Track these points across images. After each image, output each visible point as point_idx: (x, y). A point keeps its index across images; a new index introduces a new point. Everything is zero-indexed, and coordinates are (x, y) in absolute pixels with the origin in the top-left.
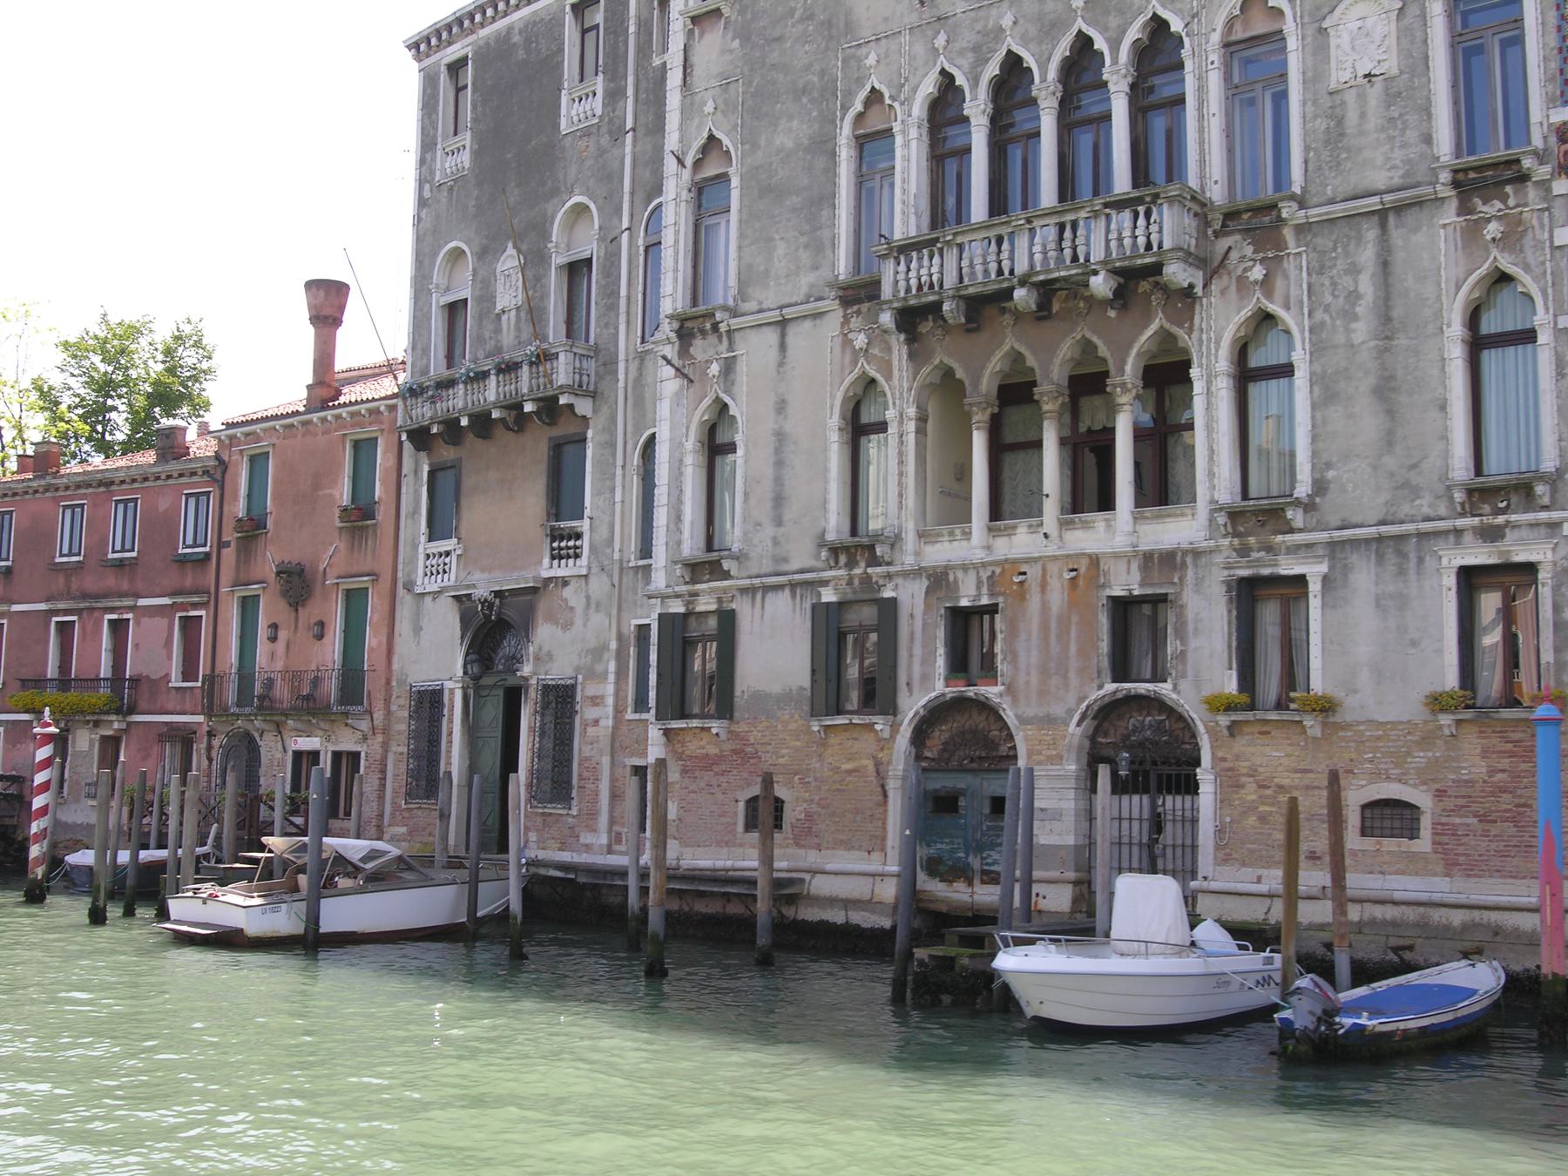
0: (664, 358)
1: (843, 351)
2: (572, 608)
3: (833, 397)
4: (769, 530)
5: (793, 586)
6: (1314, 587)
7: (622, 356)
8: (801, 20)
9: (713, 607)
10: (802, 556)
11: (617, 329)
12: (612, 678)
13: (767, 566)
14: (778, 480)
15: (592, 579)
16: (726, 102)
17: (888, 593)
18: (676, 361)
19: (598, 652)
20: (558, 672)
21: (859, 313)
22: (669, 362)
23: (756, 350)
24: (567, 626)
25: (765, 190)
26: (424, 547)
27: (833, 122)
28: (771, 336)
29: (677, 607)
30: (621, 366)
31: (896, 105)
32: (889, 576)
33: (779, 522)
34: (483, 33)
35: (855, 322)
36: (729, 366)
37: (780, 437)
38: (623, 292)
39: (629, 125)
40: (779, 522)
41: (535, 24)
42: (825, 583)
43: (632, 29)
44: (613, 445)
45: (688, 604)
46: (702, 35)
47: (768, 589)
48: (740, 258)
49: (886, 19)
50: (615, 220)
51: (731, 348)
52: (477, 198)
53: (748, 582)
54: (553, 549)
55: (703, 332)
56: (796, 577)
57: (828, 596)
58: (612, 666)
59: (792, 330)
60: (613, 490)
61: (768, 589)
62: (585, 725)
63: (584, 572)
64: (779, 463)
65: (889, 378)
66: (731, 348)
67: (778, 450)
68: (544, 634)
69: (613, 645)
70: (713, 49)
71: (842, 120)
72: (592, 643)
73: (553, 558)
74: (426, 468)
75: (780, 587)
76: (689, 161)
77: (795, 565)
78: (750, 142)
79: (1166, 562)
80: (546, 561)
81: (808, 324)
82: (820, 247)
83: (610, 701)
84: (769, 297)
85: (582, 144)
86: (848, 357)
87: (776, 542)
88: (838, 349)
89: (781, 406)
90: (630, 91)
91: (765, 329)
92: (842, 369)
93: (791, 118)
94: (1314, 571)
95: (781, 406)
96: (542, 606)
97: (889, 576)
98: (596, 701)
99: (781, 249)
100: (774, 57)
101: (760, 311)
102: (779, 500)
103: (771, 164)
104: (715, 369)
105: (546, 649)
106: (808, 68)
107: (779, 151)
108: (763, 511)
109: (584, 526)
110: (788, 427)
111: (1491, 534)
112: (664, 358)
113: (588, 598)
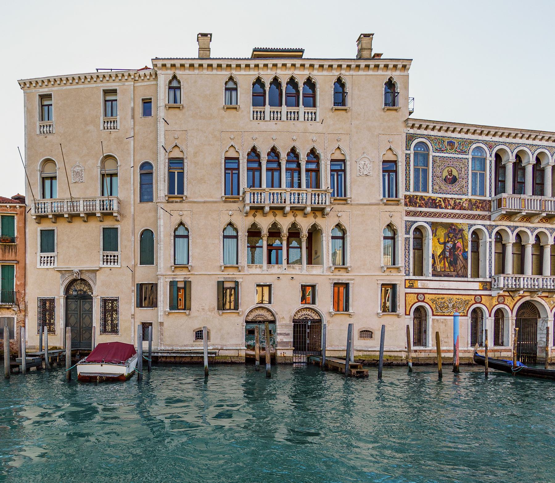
26: (39, 254)
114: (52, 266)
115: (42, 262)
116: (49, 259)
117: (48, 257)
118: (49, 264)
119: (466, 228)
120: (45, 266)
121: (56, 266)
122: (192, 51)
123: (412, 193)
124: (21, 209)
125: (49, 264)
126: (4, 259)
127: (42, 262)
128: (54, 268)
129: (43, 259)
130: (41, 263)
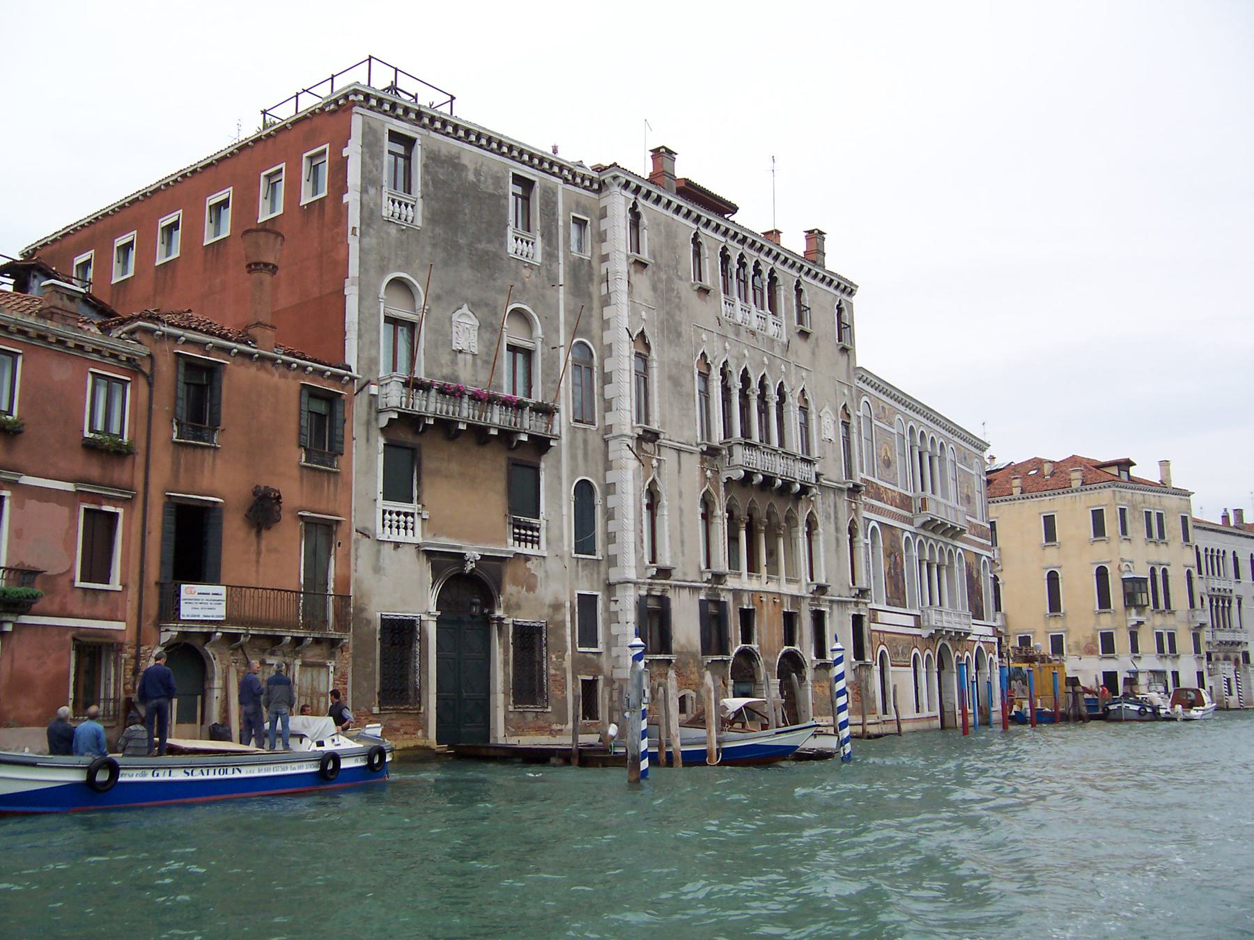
5: (690, 587)
6: (827, 616)
15: (548, 560)
26: (381, 504)
28: (674, 453)
34: (433, 134)
39: (561, 281)
42: (700, 588)
43: (561, 223)
44: (560, 478)
60: (561, 507)
64: (682, 524)
70: (643, 282)
73: (515, 539)
74: (381, 441)
79: (796, 599)
80: (511, 541)
85: (526, 272)
90: (561, 261)
94: (827, 610)
96: (508, 572)
104: (655, 463)
105: (514, 600)
109: (543, 523)
111: (857, 604)
114: (410, 538)
117: (398, 514)
119: (900, 533)
121: (418, 539)
122: (643, 167)
123: (864, 476)
126: (317, 507)
128: (418, 546)
129: (387, 515)
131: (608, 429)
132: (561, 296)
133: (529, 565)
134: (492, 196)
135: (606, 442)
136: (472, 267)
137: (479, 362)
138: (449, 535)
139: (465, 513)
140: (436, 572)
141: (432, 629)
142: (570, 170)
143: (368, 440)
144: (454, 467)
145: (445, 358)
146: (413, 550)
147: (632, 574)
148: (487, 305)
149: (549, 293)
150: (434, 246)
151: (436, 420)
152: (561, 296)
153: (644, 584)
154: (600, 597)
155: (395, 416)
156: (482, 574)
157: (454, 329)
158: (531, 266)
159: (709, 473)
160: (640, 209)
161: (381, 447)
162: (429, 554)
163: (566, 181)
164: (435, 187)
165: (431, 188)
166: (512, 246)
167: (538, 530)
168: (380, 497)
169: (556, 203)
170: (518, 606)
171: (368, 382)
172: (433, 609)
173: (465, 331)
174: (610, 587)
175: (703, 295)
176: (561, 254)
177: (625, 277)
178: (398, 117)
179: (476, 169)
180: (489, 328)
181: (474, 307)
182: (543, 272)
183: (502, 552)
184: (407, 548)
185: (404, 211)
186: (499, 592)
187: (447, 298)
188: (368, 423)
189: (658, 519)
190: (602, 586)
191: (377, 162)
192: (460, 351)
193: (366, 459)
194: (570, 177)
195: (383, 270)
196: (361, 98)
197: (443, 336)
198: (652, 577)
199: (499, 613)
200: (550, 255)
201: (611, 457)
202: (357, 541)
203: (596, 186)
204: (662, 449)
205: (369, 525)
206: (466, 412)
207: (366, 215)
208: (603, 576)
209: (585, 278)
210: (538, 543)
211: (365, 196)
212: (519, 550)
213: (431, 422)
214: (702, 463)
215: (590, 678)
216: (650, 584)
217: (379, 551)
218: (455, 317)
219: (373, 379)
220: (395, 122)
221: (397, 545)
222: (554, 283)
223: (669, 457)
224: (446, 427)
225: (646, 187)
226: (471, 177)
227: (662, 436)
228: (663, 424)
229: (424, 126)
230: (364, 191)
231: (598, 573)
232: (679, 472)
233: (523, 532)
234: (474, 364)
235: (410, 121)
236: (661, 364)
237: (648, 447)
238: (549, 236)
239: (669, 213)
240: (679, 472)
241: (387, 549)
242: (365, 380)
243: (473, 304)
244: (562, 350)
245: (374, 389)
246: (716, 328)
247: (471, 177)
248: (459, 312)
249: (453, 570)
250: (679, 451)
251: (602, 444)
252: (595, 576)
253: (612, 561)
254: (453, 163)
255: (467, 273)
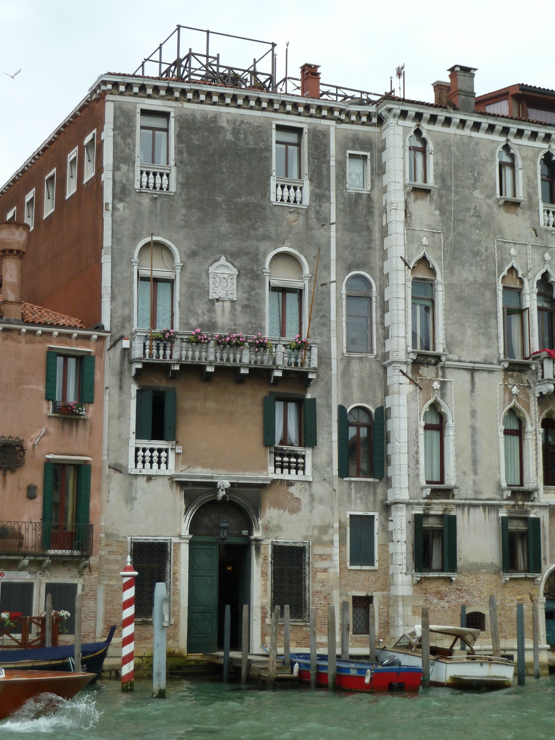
0: (401, 371)
1: (505, 393)
2: (298, 499)
3: (500, 415)
4: (471, 477)
5: (484, 506)
7: (334, 354)
8: (474, 216)
9: (440, 513)
10: (488, 493)
11: (329, 338)
12: (337, 544)
13: (470, 494)
14: (474, 451)
16: (433, 241)
17: (532, 515)
18: (410, 375)
19: (325, 529)
20: (289, 537)
21: (512, 376)
22: (404, 374)
23: (458, 381)
24: (295, 510)
25: (457, 297)
26: (133, 442)
27: (495, 275)
28: (466, 376)
29: (419, 511)
30: (334, 363)
31: (525, 280)
32: (533, 507)
33: (475, 472)
34: (187, 105)
35: (510, 380)
36: (443, 384)
37: (474, 429)
38: (333, 318)
39: (333, 219)
40: (475, 472)
41: (242, 122)
42: (500, 506)
43: (333, 163)
45: (424, 510)
46: (416, 199)
47: (471, 506)
48: (446, 330)
49: (519, 235)
50: (324, 273)
51: (443, 376)
52: (185, 215)
53: (463, 502)
54: (275, 461)
55: (428, 364)
56: (489, 502)
57: (503, 513)
58: (336, 538)
59: (477, 375)
61: (471, 506)
62: (316, 572)
63: (310, 479)
64: (474, 443)
65: (529, 411)
66: (443, 376)
67: (473, 436)
68: (270, 514)
69: (336, 525)
70: (423, 208)
71: (499, 277)
72: (318, 522)
73: (276, 467)
74: (134, 388)
75: (477, 506)
76: (411, 266)
77: (485, 496)
78: (449, 269)
80: (271, 468)
81: (485, 374)
82: (490, 339)
83: (337, 558)
84: (468, 354)
85: (292, 217)
86: (507, 397)
87: (475, 483)
88: (502, 392)
89: (473, 414)
90: (333, 200)
91: (462, 371)
92: (504, 402)
93: (471, 265)
95: (473, 414)
96: (268, 496)
97: (533, 507)
98: (322, 557)
99: (469, 332)
100: (460, 229)
101: (460, 361)
102: (475, 462)
103: (461, 285)
104: (436, 385)
105: (275, 522)
106: (479, 242)
107: (466, 280)
108: (467, 467)
110: (478, 424)
112: (401, 371)
113: (312, 496)
115: (140, 458)
116: (156, 453)
117: (152, 450)
118: (155, 465)
120: (147, 471)
121: (172, 470)
124: (100, 343)
125: (155, 465)
127: (140, 458)
128: (171, 478)
129: (140, 453)
130: (136, 462)
131: (385, 356)
132: (333, 234)
133: (292, 490)
134: (252, 151)
135: (385, 368)
136: (230, 221)
137: (238, 308)
138: (204, 466)
139: (222, 446)
140: (189, 500)
141: (185, 550)
142: (341, 111)
143: (121, 388)
144: (211, 405)
145: (201, 307)
146: (166, 482)
147: (404, 496)
148: (247, 253)
149: (319, 233)
150: (189, 207)
151: (182, 366)
152: (333, 234)
153: (418, 504)
154: (376, 517)
155: (140, 366)
156: (238, 499)
157: (211, 280)
158: (296, 211)
159: (515, 390)
160: (425, 135)
161: (134, 393)
162: (182, 484)
163: (339, 121)
164: (190, 153)
165: (185, 155)
166: (275, 194)
167: (303, 457)
168: (133, 436)
169: (327, 146)
170: (279, 528)
171: (122, 338)
172: (185, 531)
173: (223, 280)
174: (387, 508)
175: (512, 208)
176: (333, 194)
177: (402, 206)
178: (149, 96)
179: (234, 129)
180: (250, 274)
181: (232, 257)
182: (312, 215)
183: (257, 479)
184: (160, 481)
185: (151, 181)
186: (257, 516)
187: (202, 252)
188: (121, 373)
189: (445, 439)
190: (379, 507)
191: (129, 140)
192: (218, 300)
193: (117, 407)
194: (343, 117)
195: (136, 238)
196: (109, 87)
197: (198, 289)
198: (428, 497)
199: (257, 534)
200: (319, 197)
201: (389, 383)
202: (109, 477)
203: (375, 120)
204: (448, 372)
205: (122, 462)
206: (211, 356)
207: (118, 190)
208: (380, 497)
209: (362, 213)
210: (303, 469)
211: (117, 174)
212: (281, 477)
213: (177, 368)
214: (505, 379)
215: (363, 594)
216: (426, 504)
217: (131, 484)
218: (212, 269)
219: (126, 333)
220: (147, 101)
221: (149, 478)
222: (324, 222)
223: (452, 377)
224: (193, 370)
225: (427, 113)
226: (229, 137)
227: (443, 359)
228: (449, 346)
229: (177, 100)
230: (116, 168)
231: (375, 494)
232: (472, 391)
233: (286, 459)
234: (233, 309)
235: (162, 98)
236: (449, 287)
237: (427, 372)
238: (319, 178)
239: (467, 132)
240: (472, 391)
241: (141, 481)
242: (118, 336)
243: (232, 255)
244: (333, 286)
245: (126, 344)
246: (532, 240)
247: (229, 137)
248: (217, 264)
249: (207, 497)
250: (472, 371)
251: (381, 371)
252: (371, 498)
253: (388, 483)
254: (210, 125)
255: (224, 227)
